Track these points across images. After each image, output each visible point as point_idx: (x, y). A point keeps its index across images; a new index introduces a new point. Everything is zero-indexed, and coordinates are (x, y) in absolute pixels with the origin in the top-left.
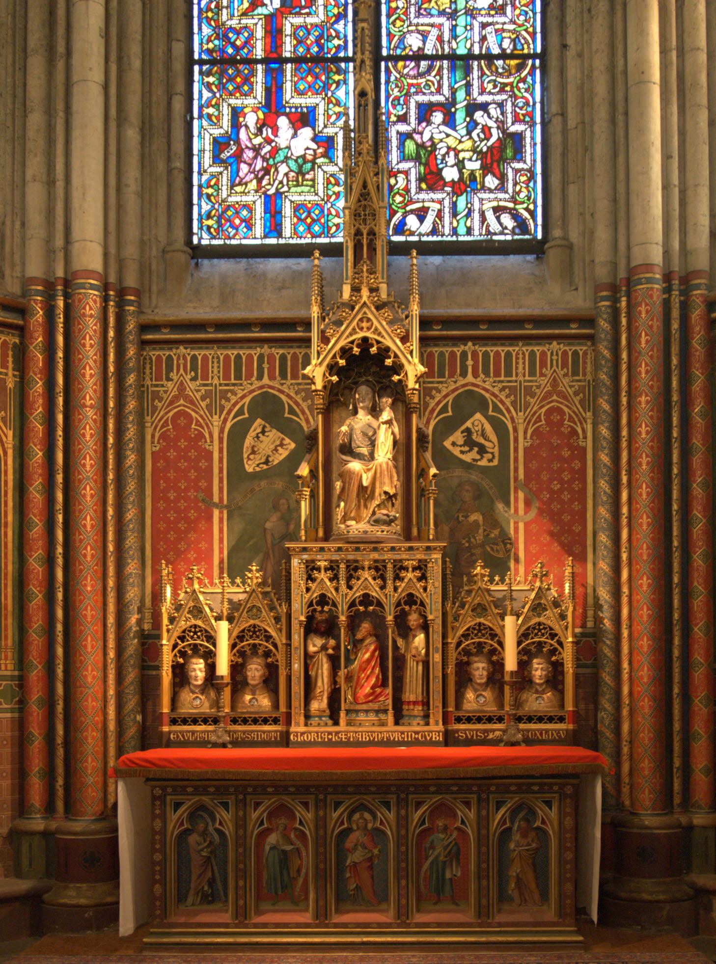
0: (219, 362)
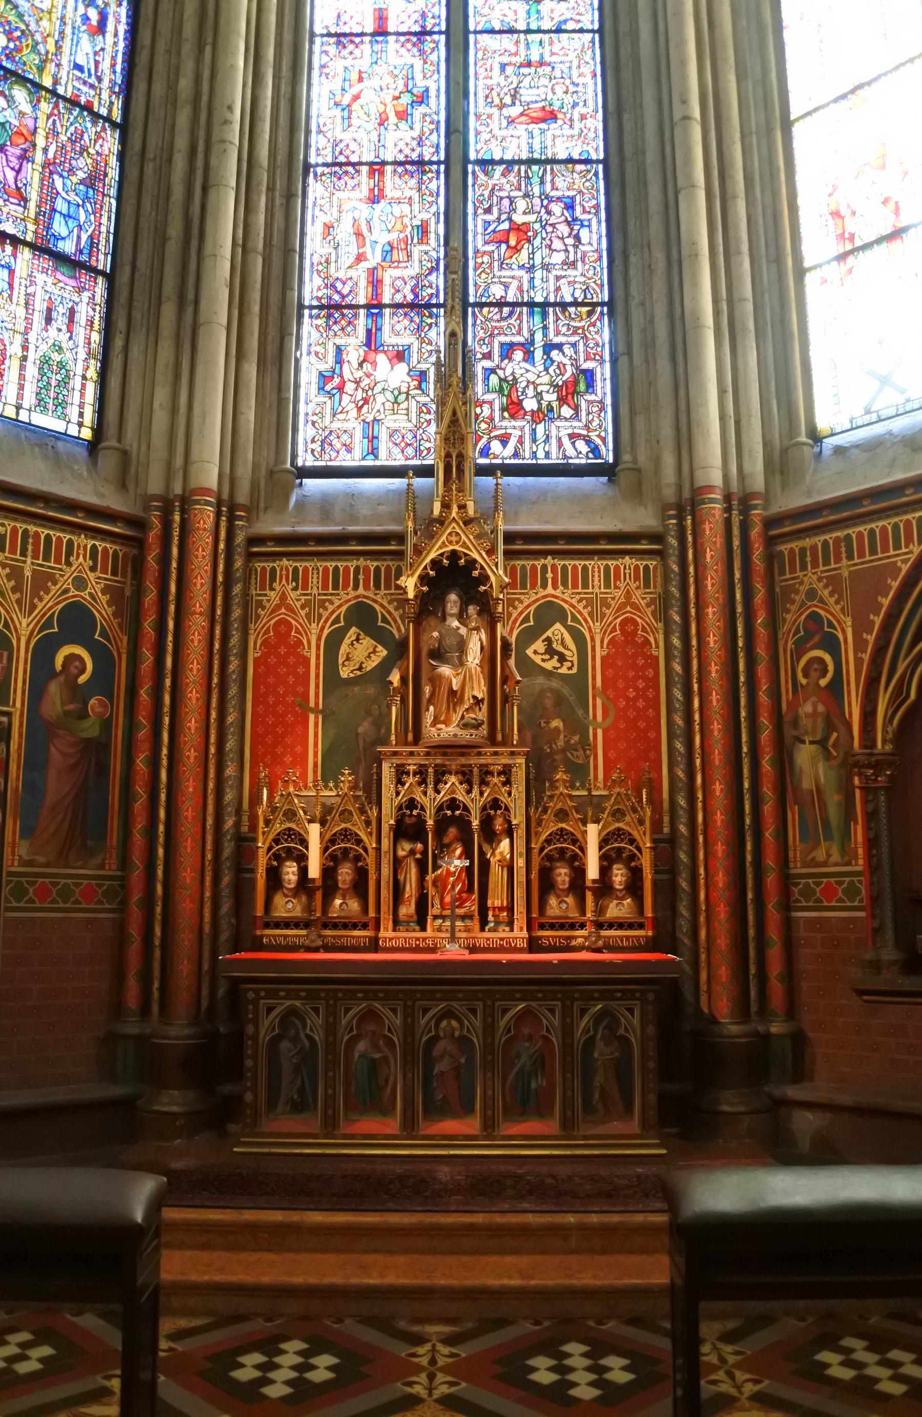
0: (318, 573)
